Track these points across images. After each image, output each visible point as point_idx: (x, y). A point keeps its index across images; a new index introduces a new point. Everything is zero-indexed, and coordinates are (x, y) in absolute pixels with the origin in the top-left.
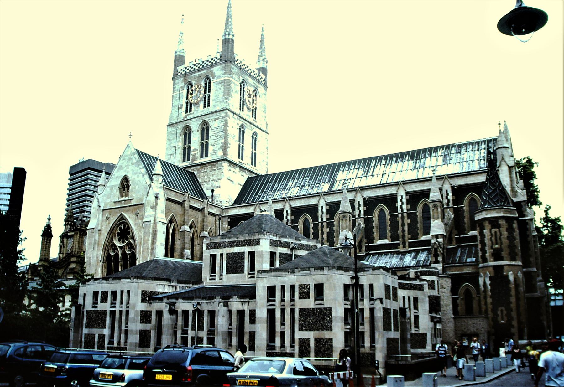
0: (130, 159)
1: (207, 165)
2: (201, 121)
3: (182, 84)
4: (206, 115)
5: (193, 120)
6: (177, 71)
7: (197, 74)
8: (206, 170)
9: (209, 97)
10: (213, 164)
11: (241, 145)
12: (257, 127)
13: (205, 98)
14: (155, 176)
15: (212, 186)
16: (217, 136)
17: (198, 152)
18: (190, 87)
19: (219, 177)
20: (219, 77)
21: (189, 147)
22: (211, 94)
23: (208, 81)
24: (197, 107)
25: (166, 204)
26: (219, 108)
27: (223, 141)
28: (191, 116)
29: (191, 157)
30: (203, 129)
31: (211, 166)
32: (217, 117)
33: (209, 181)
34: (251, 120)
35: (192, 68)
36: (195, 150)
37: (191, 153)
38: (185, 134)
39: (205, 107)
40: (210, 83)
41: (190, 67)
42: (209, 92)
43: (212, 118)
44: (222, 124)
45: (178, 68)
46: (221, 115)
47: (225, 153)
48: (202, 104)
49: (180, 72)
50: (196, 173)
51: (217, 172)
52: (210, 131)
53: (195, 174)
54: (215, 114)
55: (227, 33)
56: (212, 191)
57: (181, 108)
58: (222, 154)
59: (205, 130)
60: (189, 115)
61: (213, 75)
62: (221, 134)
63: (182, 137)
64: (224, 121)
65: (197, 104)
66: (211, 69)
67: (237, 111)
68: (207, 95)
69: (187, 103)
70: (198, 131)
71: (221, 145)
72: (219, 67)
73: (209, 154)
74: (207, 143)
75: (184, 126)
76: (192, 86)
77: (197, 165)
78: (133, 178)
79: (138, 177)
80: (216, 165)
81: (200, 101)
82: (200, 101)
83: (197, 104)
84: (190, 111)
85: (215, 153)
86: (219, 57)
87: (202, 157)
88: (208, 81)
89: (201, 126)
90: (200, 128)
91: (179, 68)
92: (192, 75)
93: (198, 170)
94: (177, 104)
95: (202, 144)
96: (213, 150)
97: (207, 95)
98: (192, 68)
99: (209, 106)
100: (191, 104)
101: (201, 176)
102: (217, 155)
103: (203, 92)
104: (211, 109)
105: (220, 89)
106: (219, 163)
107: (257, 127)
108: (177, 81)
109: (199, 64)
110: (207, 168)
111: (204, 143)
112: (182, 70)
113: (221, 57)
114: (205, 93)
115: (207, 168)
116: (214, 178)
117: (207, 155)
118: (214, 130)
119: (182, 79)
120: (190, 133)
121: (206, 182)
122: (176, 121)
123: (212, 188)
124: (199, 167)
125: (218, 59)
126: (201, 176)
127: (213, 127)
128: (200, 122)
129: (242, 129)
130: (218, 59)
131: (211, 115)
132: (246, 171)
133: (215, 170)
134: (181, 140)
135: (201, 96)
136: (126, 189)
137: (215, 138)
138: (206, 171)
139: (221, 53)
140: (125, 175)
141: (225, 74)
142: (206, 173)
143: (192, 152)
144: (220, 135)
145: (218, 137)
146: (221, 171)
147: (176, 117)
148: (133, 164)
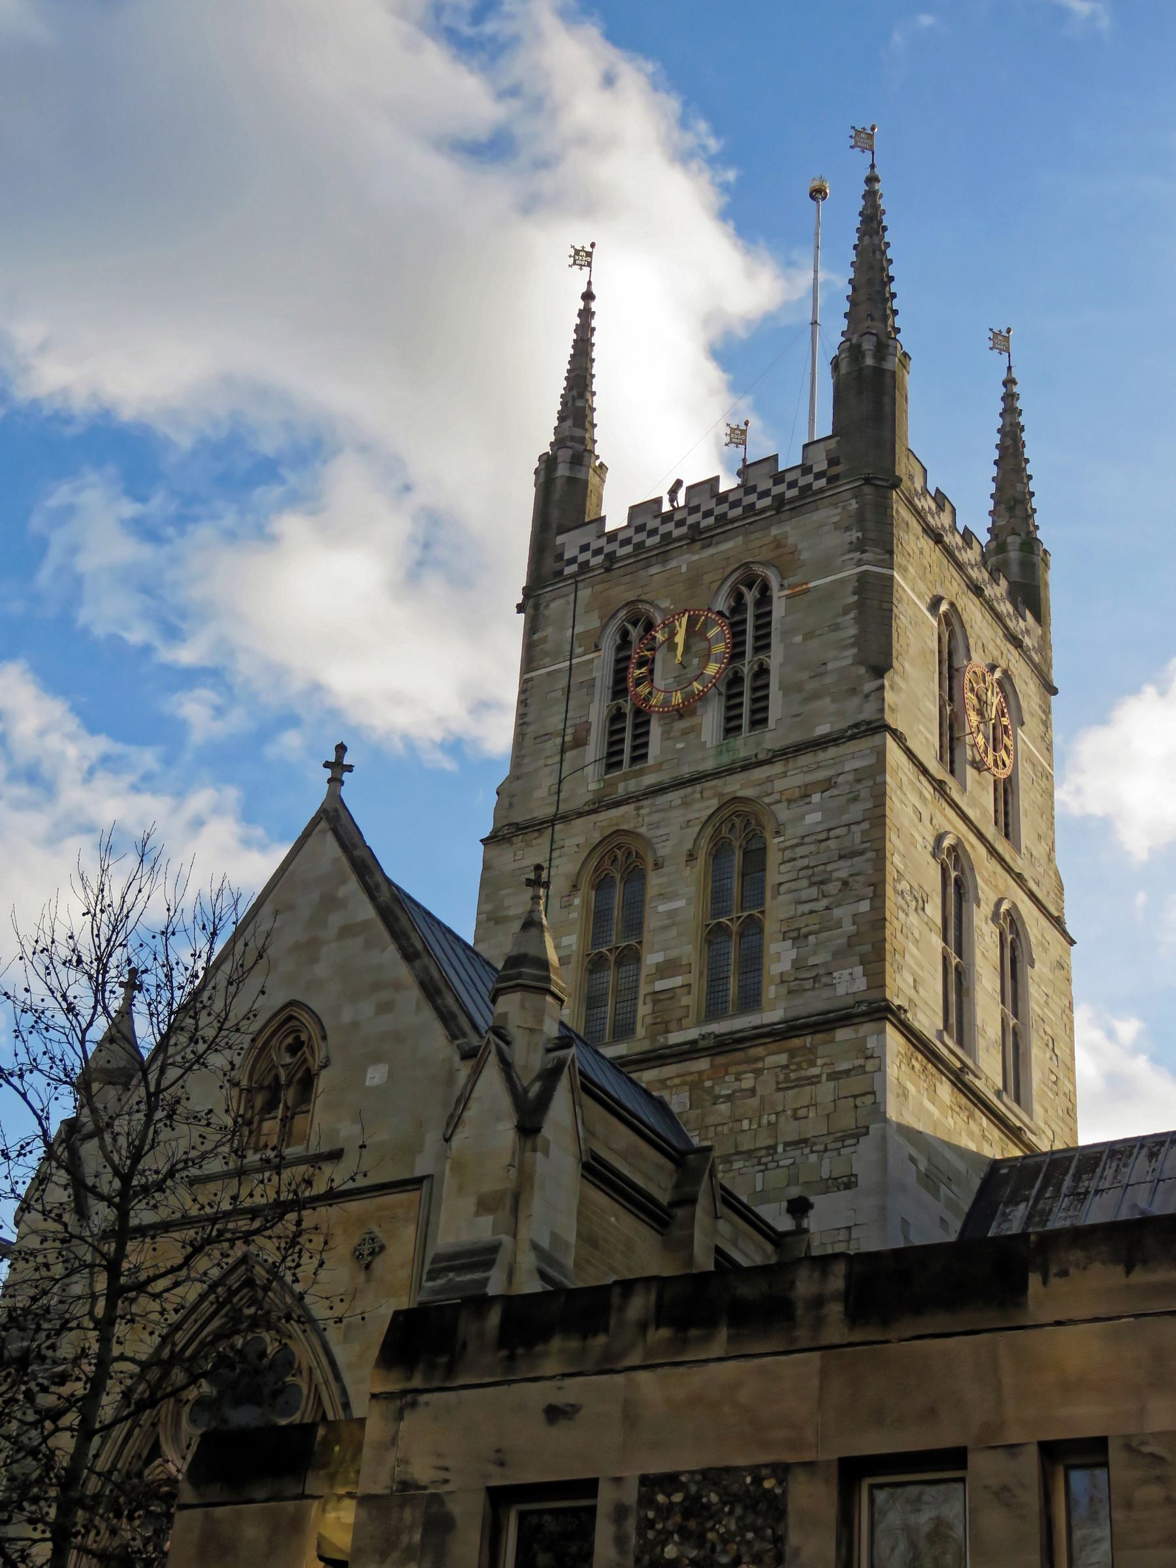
0: (329, 902)
1: (759, 1051)
2: (714, 803)
3: (590, 622)
4: (744, 768)
5: (661, 800)
6: (560, 557)
7: (683, 562)
8: (748, 1082)
9: (762, 671)
10: (796, 1042)
11: (955, 960)
12: (1019, 878)
13: (735, 680)
14: (516, 997)
15: (793, 1180)
16: (822, 883)
17: (692, 978)
18: (635, 633)
19: (846, 1121)
20: (825, 567)
21: (630, 956)
22: (776, 658)
23: (750, 597)
24: (685, 733)
25: (583, 1201)
26: (823, 729)
27: (865, 906)
28: (649, 780)
29: (644, 1010)
30: (719, 850)
31: (783, 1059)
32: (821, 775)
33: (774, 1147)
34: (990, 831)
35: (652, 533)
36: (667, 969)
37: (644, 989)
38: (602, 884)
39: (731, 729)
40: (765, 598)
41: (640, 529)
42: (762, 644)
43: (779, 785)
44: (856, 811)
45: (560, 539)
46: (849, 766)
47: (877, 979)
48: (711, 720)
49: (573, 560)
50: (678, 1102)
51: (826, 1091)
52: (773, 858)
53: (675, 1109)
54: (806, 760)
55: (868, 345)
56: (799, 1207)
57: (580, 742)
58: (861, 984)
59: (737, 858)
60: (626, 778)
61: (785, 561)
62: (842, 870)
63: (586, 903)
64: (864, 793)
65: (681, 713)
66: (774, 531)
67: (933, 766)
68: (747, 668)
69: (617, 716)
70: (691, 857)
71: (849, 928)
72: (827, 515)
73: (771, 991)
74: (753, 927)
75: (597, 837)
76: (650, 626)
77: (690, 1051)
78: (347, 1016)
79: (385, 1008)
80: (821, 1051)
81: (702, 697)
82: (702, 697)
83: (681, 713)
84: (639, 757)
85: (816, 978)
86: (821, 466)
87: (714, 1009)
88: (750, 597)
89: (709, 830)
90: (703, 843)
91: (570, 543)
92: (654, 570)
93: (695, 1086)
94: (554, 722)
95: (714, 934)
96: (797, 965)
97: (747, 668)
98: (652, 533)
99: (760, 720)
100: (642, 720)
101: (711, 1120)
102: (827, 993)
103: (720, 648)
104: (773, 737)
105: (836, 627)
106: (843, 1034)
107: (1019, 878)
108: (556, 607)
109: (696, 509)
110: (758, 1072)
111: (735, 928)
112: (585, 548)
113: (833, 462)
114: (736, 654)
115: (758, 1072)
116: (814, 1127)
117: (750, 1000)
118: (801, 851)
119: (585, 594)
120: (635, 875)
121: (749, 1153)
122: (546, 811)
123: (795, 1192)
124: (703, 1064)
125: (819, 476)
126: (711, 1120)
127: (793, 833)
128: (704, 805)
129: (953, 874)
130: (819, 476)
131: (778, 768)
132: (985, 1121)
133: (814, 1081)
134: (574, 915)
135: (712, 669)
136: (289, 1096)
137: (814, 892)
138: (753, 1091)
139: (832, 444)
140: (292, 1003)
141: (859, 546)
142: (754, 1102)
143: (652, 979)
144: (843, 874)
145: (833, 888)
146: (855, 1085)
147: (542, 792)
148: (346, 931)
